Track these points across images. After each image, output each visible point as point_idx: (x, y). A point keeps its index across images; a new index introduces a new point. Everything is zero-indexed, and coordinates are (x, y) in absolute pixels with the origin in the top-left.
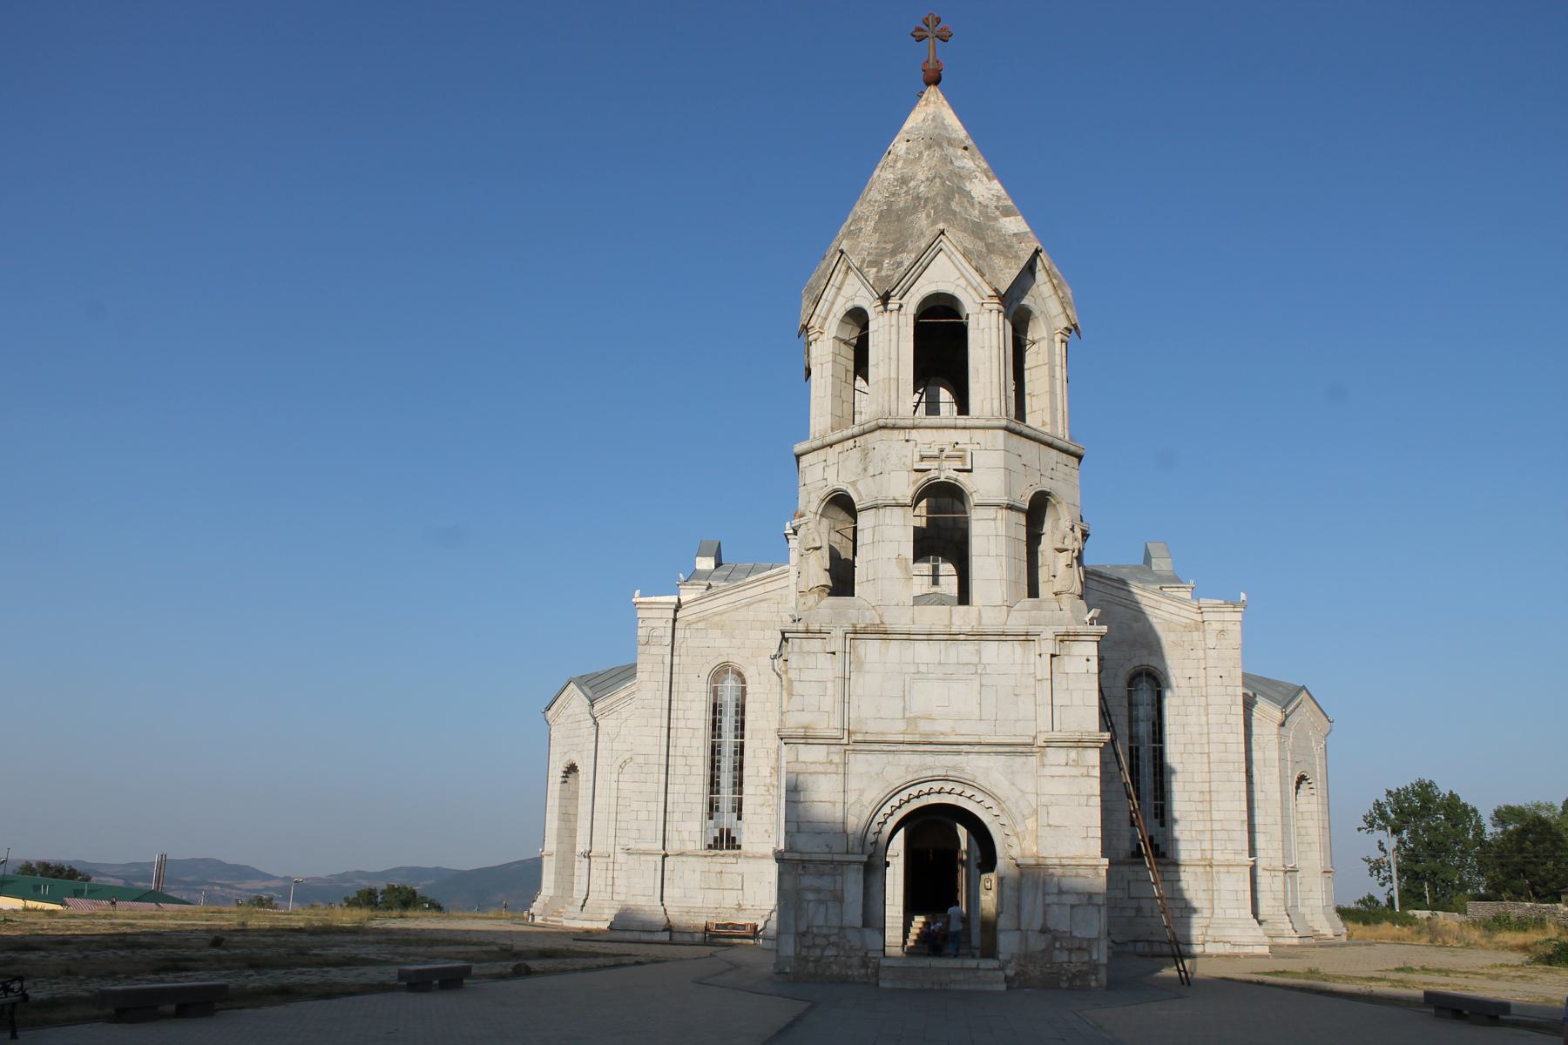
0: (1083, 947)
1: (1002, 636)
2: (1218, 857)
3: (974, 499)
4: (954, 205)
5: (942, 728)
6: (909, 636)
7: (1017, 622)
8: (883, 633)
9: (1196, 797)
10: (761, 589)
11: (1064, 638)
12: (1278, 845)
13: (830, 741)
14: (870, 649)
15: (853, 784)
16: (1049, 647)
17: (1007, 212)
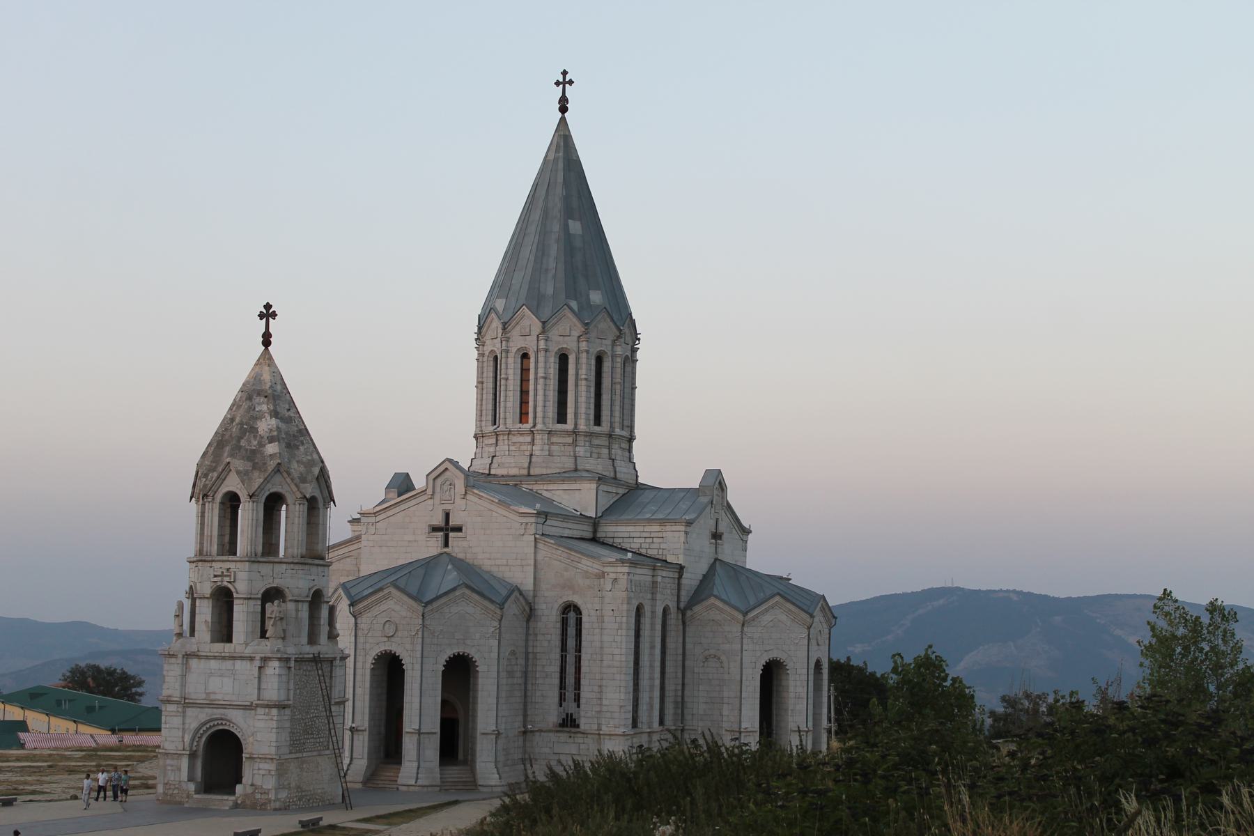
0: (266, 792)
1: (242, 658)
2: (605, 729)
3: (235, 595)
4: (243, 443)
5: (219, 697)
6: (207, 657)
7: (248, 651)
8: (196, 655)
9: (596, 689)
10: (346, 550)
11: (265, 660)
12: (736, 712)
13: (178, 703)
14: (194, 663)
15: (188, 721)
16: (257, 663)
17: (271, 440)
